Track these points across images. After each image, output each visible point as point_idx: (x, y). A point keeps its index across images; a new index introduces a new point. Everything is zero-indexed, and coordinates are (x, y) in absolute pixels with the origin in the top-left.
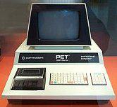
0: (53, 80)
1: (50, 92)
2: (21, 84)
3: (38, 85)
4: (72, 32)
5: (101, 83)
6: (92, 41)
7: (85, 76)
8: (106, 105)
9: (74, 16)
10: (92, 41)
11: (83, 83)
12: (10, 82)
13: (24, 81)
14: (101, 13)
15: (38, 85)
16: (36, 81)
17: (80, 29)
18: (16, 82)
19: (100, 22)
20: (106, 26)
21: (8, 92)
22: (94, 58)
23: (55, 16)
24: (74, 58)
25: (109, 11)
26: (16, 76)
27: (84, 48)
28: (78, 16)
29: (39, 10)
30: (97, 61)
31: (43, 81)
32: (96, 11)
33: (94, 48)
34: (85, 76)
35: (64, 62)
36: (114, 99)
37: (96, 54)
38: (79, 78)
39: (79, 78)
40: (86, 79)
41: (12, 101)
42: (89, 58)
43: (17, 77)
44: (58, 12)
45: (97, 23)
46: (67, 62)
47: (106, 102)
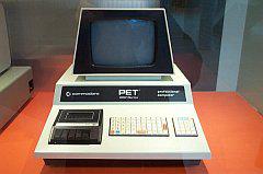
0: (114, 128)
1: (109, 147)
2: (64, 135)
3: (91, 137)
4: (144, 52)
5: (189, 133)
6: (175, 67)
7: (164, 122)
8: (197, 167)
9: (147, 28)
10: (175, 67)
11: (161, 133)
12: (47, 132)
13: (69, 130)
14: (189, 24)
15: (91, 137)
16: (87, 131)
17: (156, 48)
18: (57, 131)
19: (186, 37)
20: (197, 44)
21: (45, 147)
22: (178, 94)
23: (117, 27)
24: (148, 95)
25: (202, 20)
26: (56, 121)
27: (163, 79)
28: (153, 30)
29: (93, 19)
30: (183, 99)
31: (99, 130)
32: (181, 20)
33: (178, 78)
34: (164, 122)
35: (130, 100)
36: (210, 158)
37: (181, 88)
38: (154, 125)
39: (154, 125)
40: (165, 127)
41: (52, 162)
42: (171, 94)
43: (58, 125)
44: (121, 22)
45: (183, 38)
46: (136, 100)
47: (196, 163)
